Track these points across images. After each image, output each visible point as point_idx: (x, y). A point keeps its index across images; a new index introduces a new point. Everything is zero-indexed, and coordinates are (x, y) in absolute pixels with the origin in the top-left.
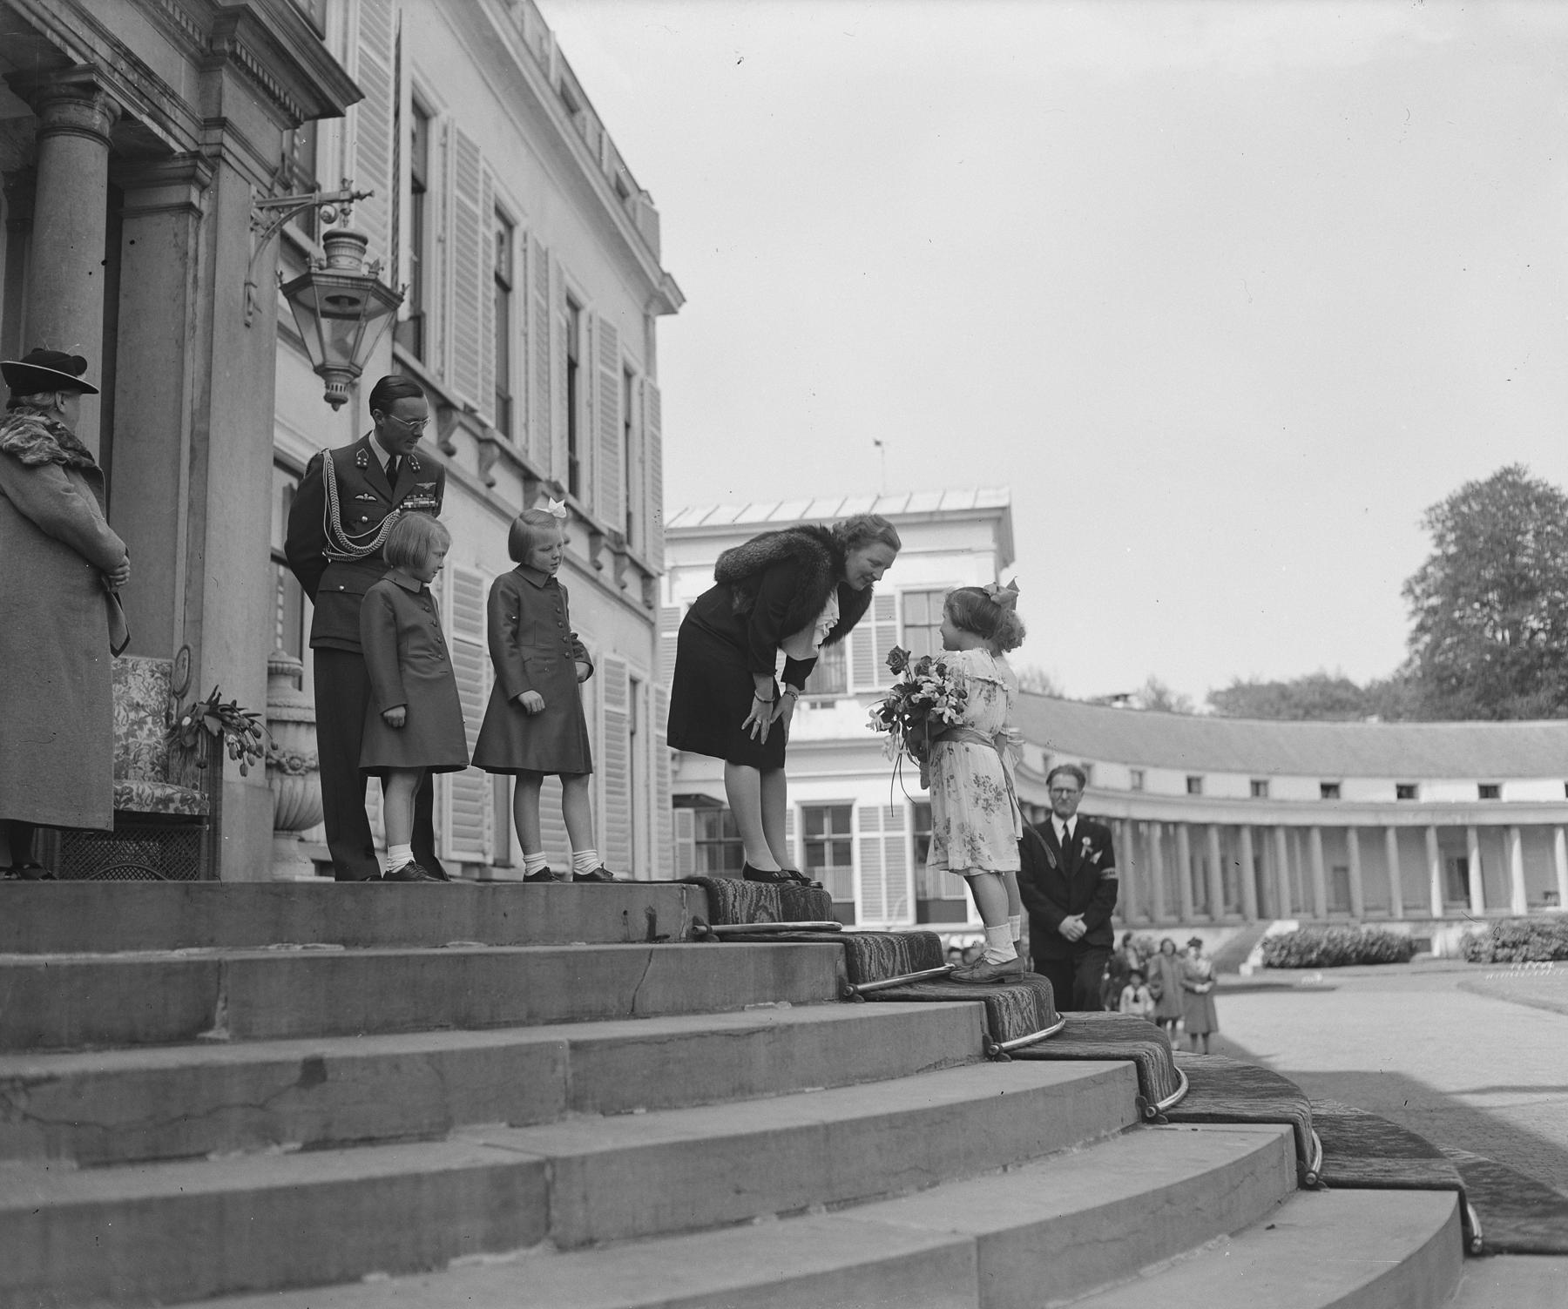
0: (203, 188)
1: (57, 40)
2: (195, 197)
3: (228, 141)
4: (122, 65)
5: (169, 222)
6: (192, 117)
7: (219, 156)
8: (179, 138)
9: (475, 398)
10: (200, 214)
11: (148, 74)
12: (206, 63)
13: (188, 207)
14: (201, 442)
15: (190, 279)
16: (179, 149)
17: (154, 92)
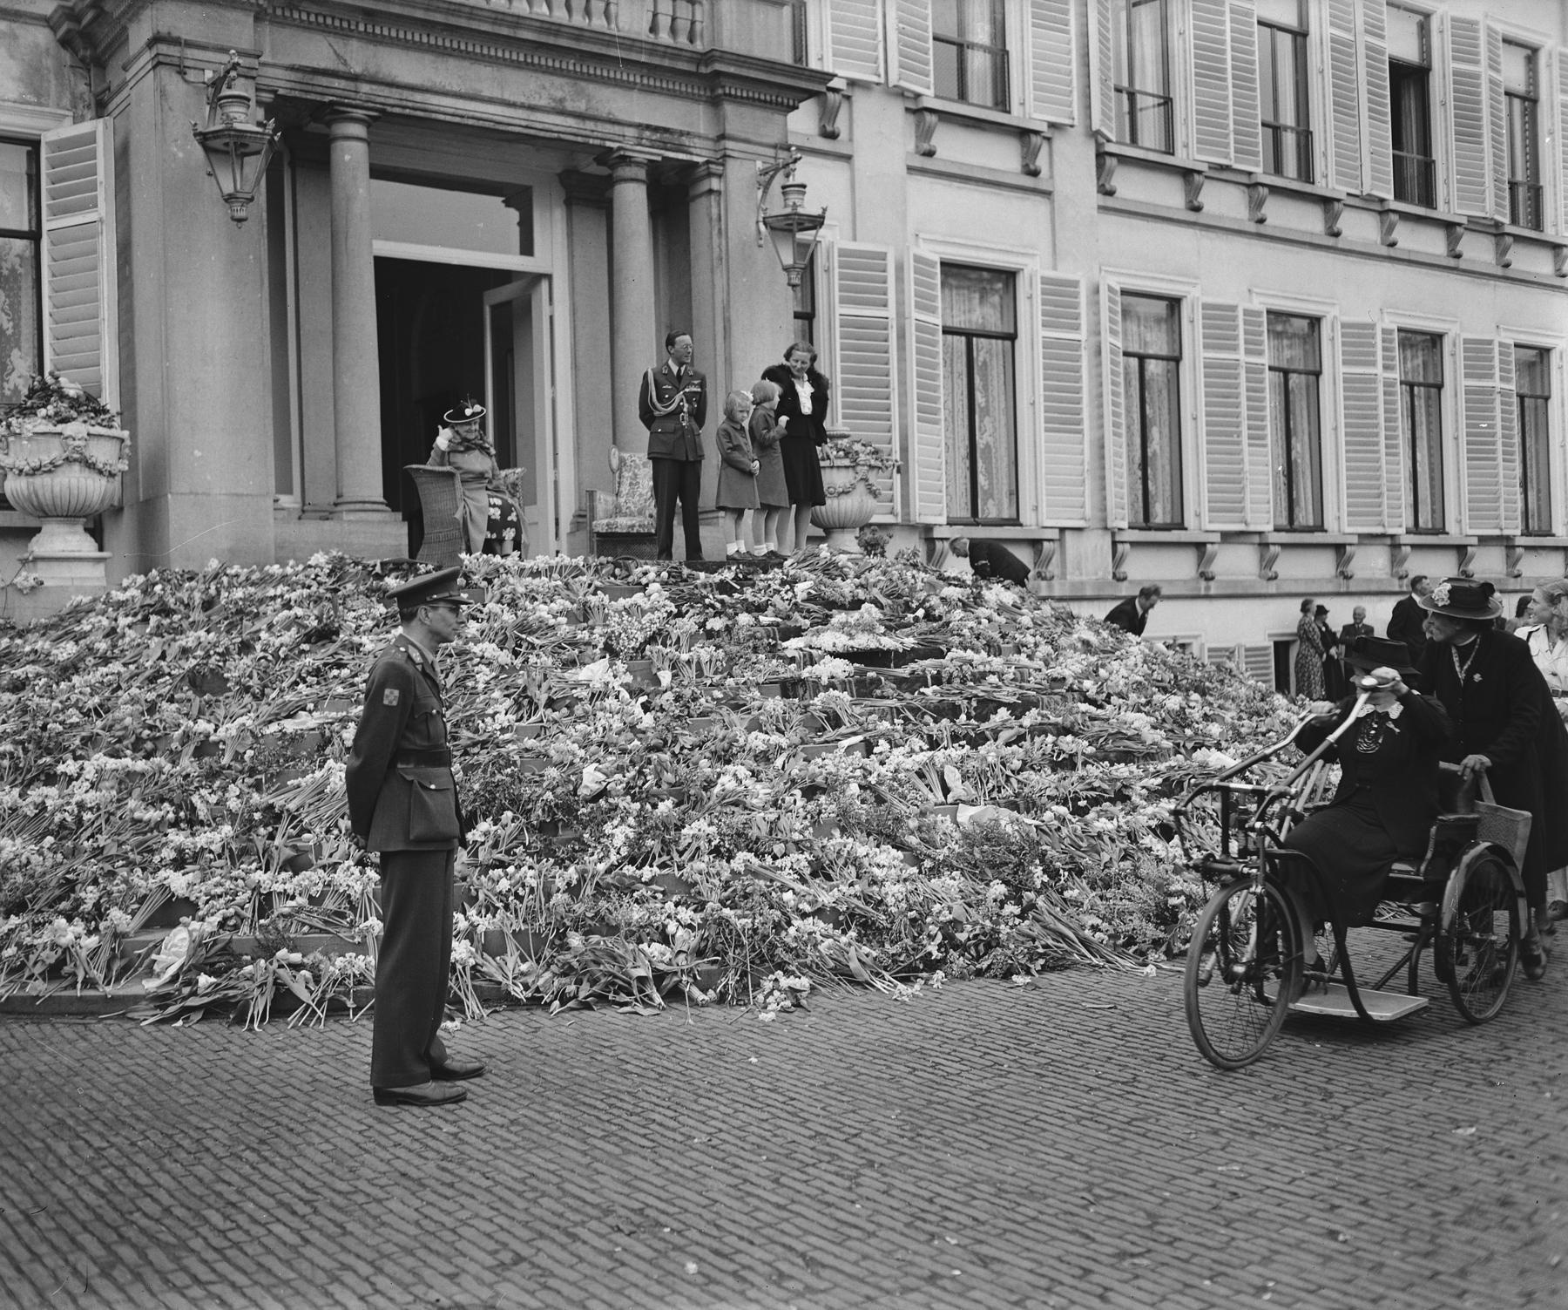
0: (720, 176)
1: (597, 142)
2: (715, 184)
3: (729, 144)
4: (647, 134)
5: (703, 200)
6: (707, 139)
7: (725, 156)
8: (699, 154)
9: (1227, 156)
10: (719, 192)
11: (666, 130)
12: (715, 102)
13: (710, 191)
14: (727, 322)
15: (715, 232)
16: (700, 160)
17: (675, 139)
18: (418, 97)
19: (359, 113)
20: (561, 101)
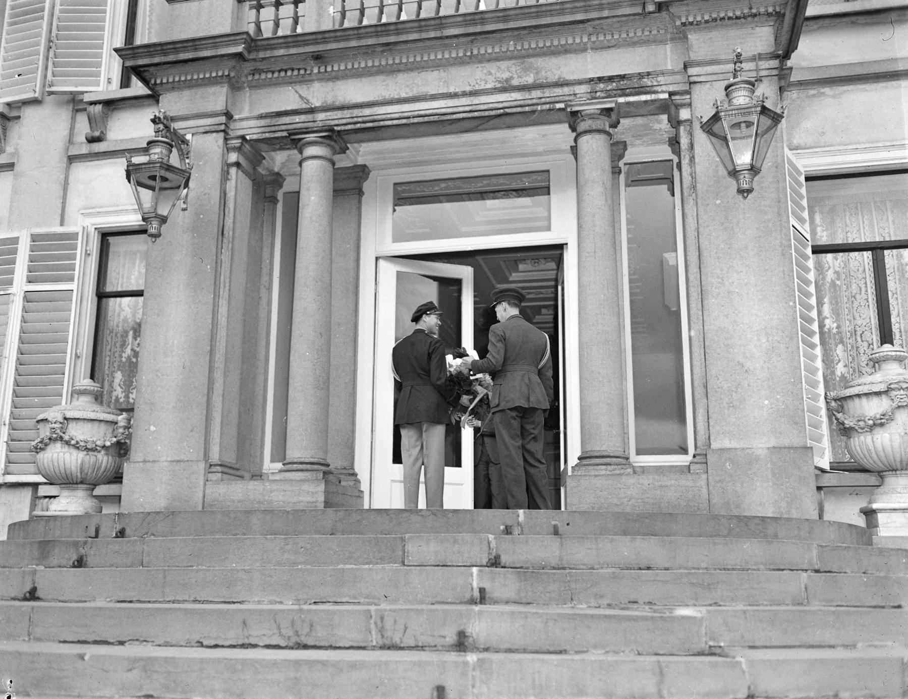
1: (548, 106)
18: (367, 112)
19: (311, 137)
20: (507, 80)
